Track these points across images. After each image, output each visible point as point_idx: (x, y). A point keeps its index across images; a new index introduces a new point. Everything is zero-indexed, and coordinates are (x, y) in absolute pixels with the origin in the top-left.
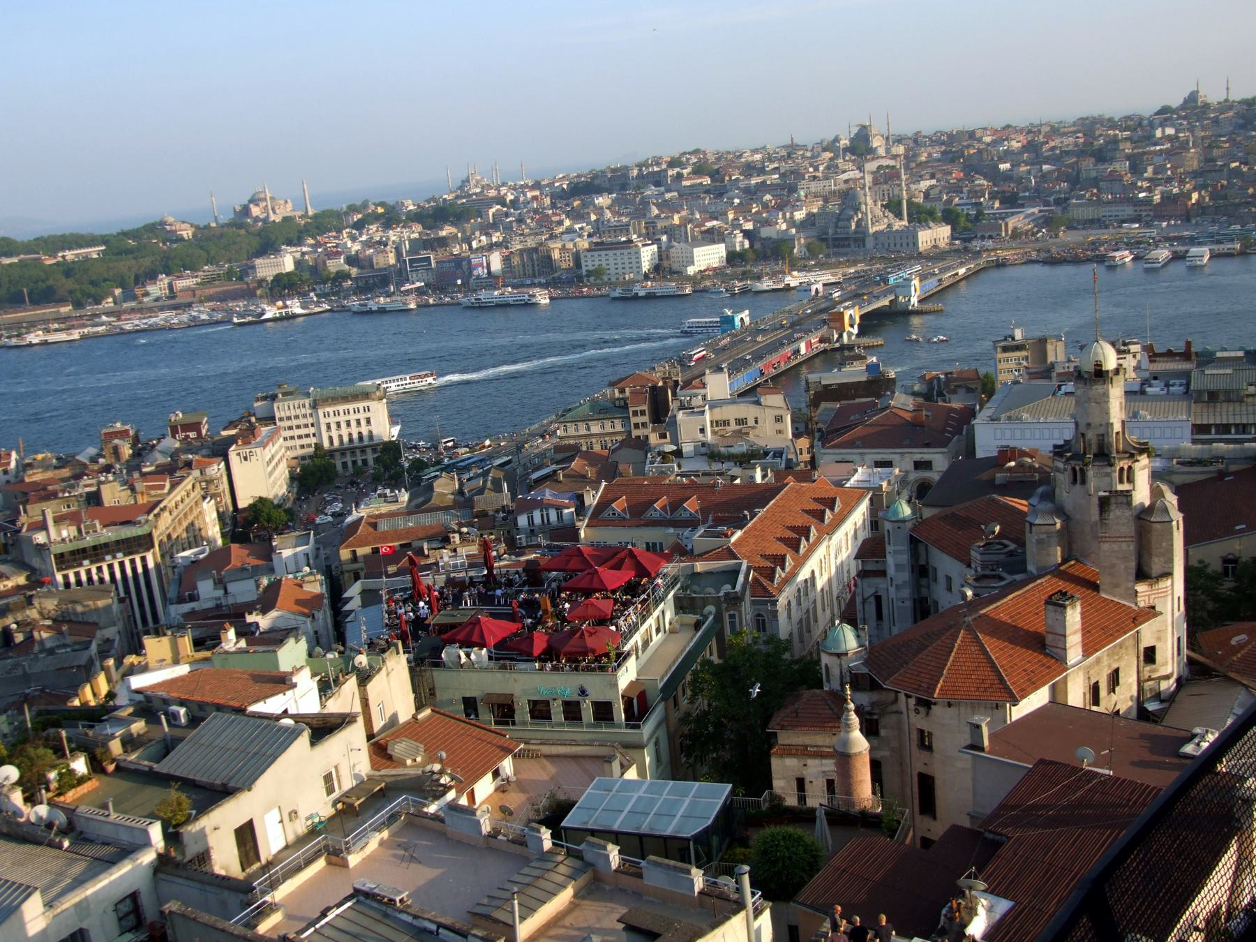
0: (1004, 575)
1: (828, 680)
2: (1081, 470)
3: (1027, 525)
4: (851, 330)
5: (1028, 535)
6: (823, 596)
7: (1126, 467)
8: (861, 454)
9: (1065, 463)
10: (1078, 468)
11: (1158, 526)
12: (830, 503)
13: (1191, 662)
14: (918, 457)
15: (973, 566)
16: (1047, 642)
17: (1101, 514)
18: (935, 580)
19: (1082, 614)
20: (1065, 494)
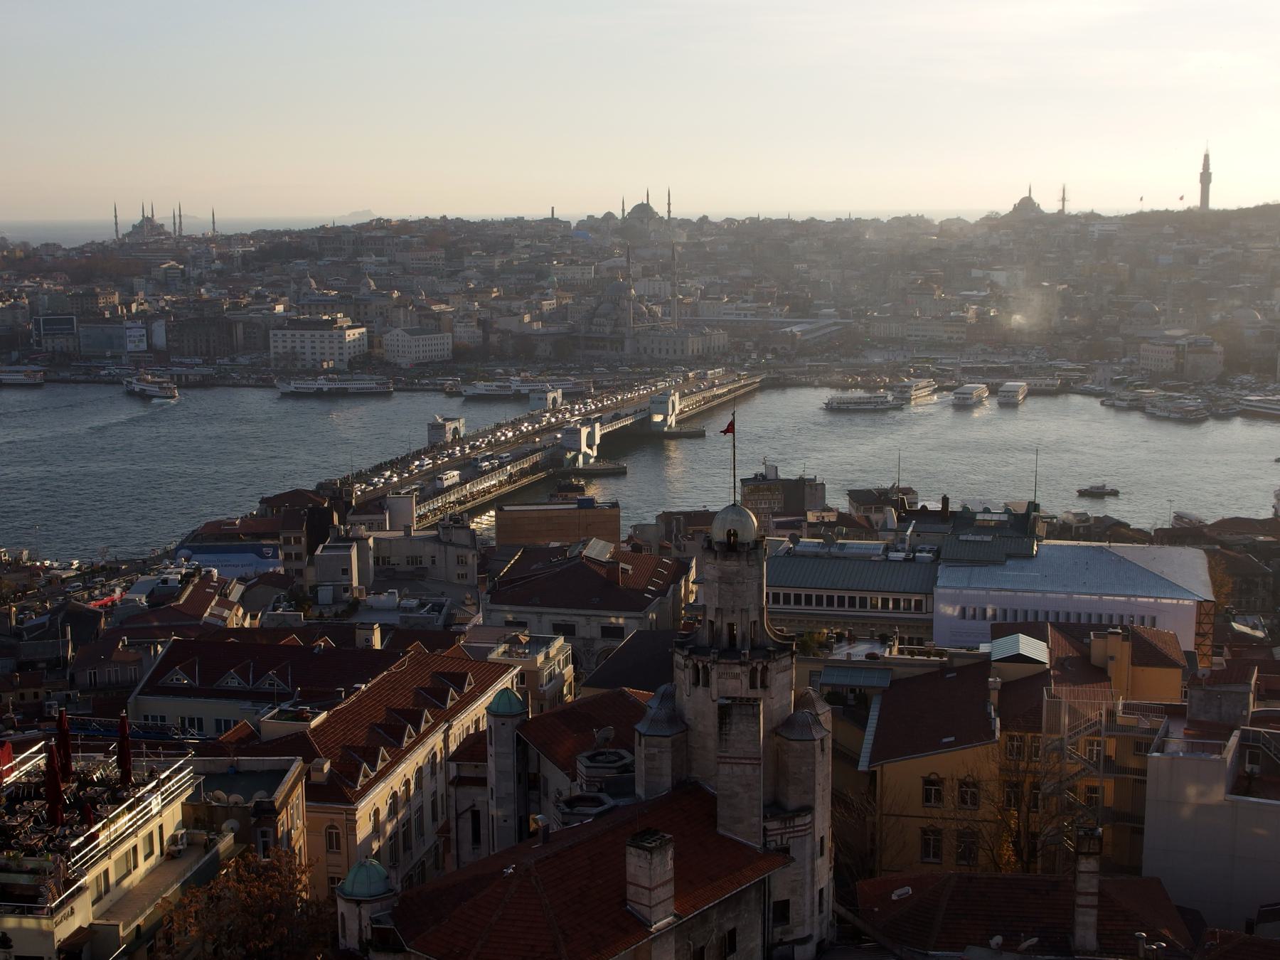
0: (603, 796)
1: (344, 937)
2: (705, 667)
3: (637, 735)
4: (589, 451)
5: (637, 748)
6: (434, 803)
7: (760, 668)
8: (537, 613)
9: (686, 658)
10: (700, 666)
11: (796, 745)
12: (459, 680)
13: (840, 920)
14: (605, 621)
15: (579, 781)
16: (629, 896)
17: (720, 728)
18: (546, 795)
19: (675, 860)
20: (685, 696)
